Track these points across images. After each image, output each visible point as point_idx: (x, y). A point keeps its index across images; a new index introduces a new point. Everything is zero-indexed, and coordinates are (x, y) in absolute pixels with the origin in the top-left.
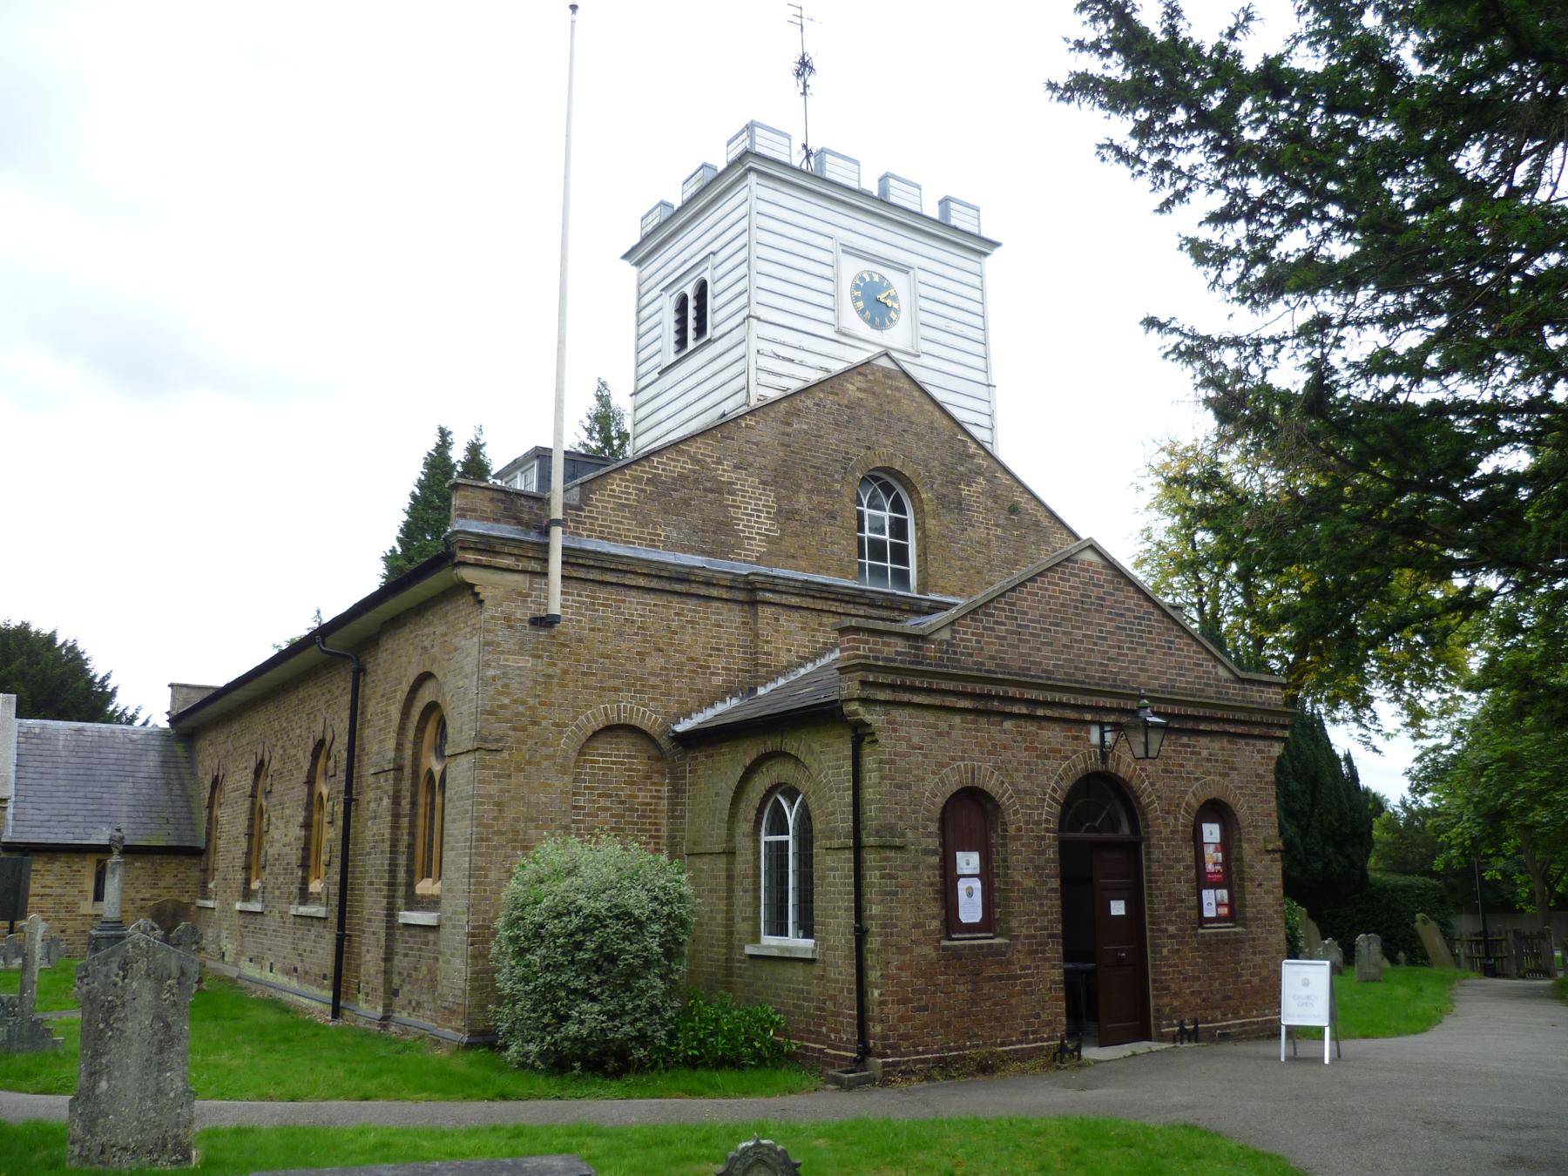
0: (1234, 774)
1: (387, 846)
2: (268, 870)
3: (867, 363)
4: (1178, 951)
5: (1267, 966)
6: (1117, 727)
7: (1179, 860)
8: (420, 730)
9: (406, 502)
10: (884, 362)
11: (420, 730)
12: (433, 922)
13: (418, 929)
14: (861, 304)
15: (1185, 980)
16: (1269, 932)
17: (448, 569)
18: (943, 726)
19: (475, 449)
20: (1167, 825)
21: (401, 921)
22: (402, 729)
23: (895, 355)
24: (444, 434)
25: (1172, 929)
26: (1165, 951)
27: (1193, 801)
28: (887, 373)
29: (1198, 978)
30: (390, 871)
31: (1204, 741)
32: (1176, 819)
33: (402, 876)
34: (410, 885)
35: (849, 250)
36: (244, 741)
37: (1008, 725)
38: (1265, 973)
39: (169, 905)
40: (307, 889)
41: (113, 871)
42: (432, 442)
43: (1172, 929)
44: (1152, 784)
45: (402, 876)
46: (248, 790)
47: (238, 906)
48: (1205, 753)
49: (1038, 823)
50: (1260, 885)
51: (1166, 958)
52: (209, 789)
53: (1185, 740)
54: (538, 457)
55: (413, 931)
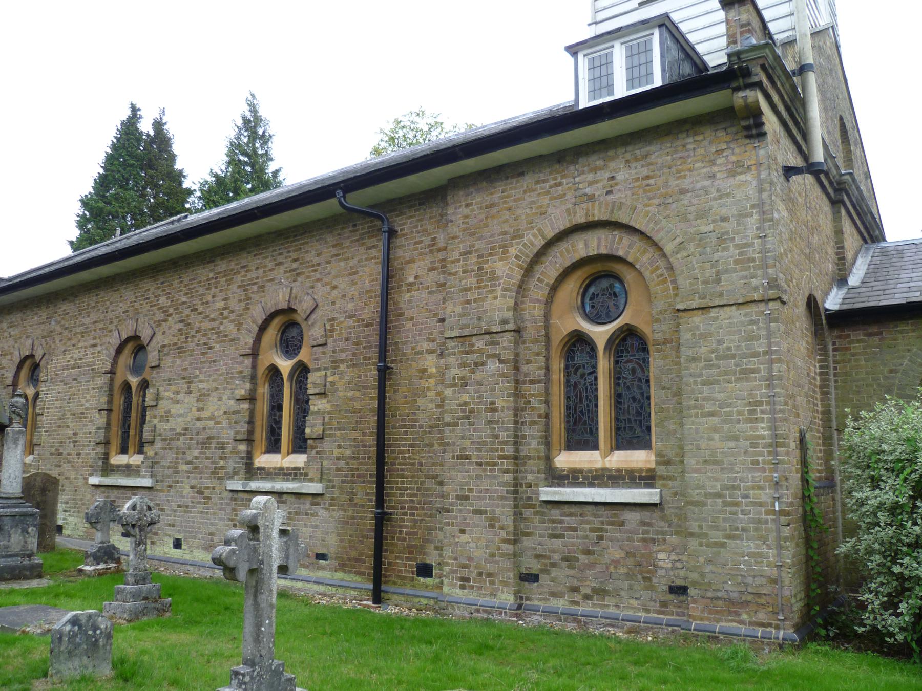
1: (507, 417)
2: (159, 444)
8: (554, 288)
9: (101, 158)
11: (554, 288)
12: (656, 499)
13: (590, 508)
17: (728, 92)
19: (158, 125)
21: (543, 498)
22: (521, 288)
24: (134, 109)
30: (516, 443)
33: (533, 446)
34: (548, 459)
36: (87, 321)
39: (38, 479)
40: (252, 464)
41: (16, 441)
42: (126, 114)
45: (533, 446)
46: (108, 366)
47: (94, 480)
52: (14, 369)
54: (660, 26)
55: (567, 509)
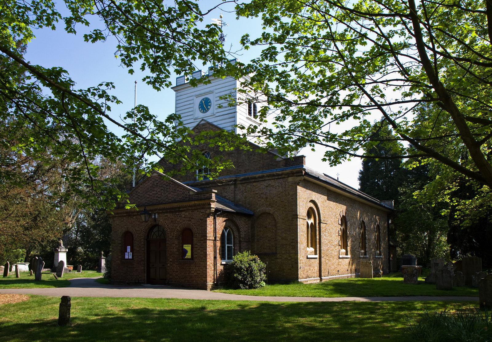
0: (192, 220)
3: (198, 125)
4: (172, 265)
5: (200, 270)
6: (159, 213)
7: (173, 243)
10: (203, 122)
14: (200, 109)
15: (174, 272)
16: (201, 261)
18: (122, 220)
20: (171, 235)
23: (205, 119)
25: (171, 260)
26: (169, 265)
27: (179, 228)
28: (203, 125)
29: (178, 272)
31: (183, 213)
32: (174, 233)
35: (197, 96)
37: (134, 217)
38: (199, 272)
43: (171, 260)
44: (168, 226)
48: (183, 216)
49: (140, 237)
50: (199, 249)
51: (169, 266)
53: (177, 213)
